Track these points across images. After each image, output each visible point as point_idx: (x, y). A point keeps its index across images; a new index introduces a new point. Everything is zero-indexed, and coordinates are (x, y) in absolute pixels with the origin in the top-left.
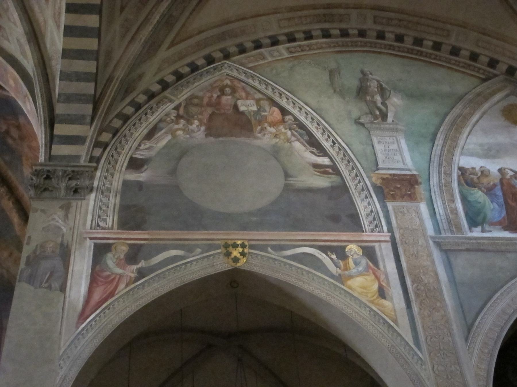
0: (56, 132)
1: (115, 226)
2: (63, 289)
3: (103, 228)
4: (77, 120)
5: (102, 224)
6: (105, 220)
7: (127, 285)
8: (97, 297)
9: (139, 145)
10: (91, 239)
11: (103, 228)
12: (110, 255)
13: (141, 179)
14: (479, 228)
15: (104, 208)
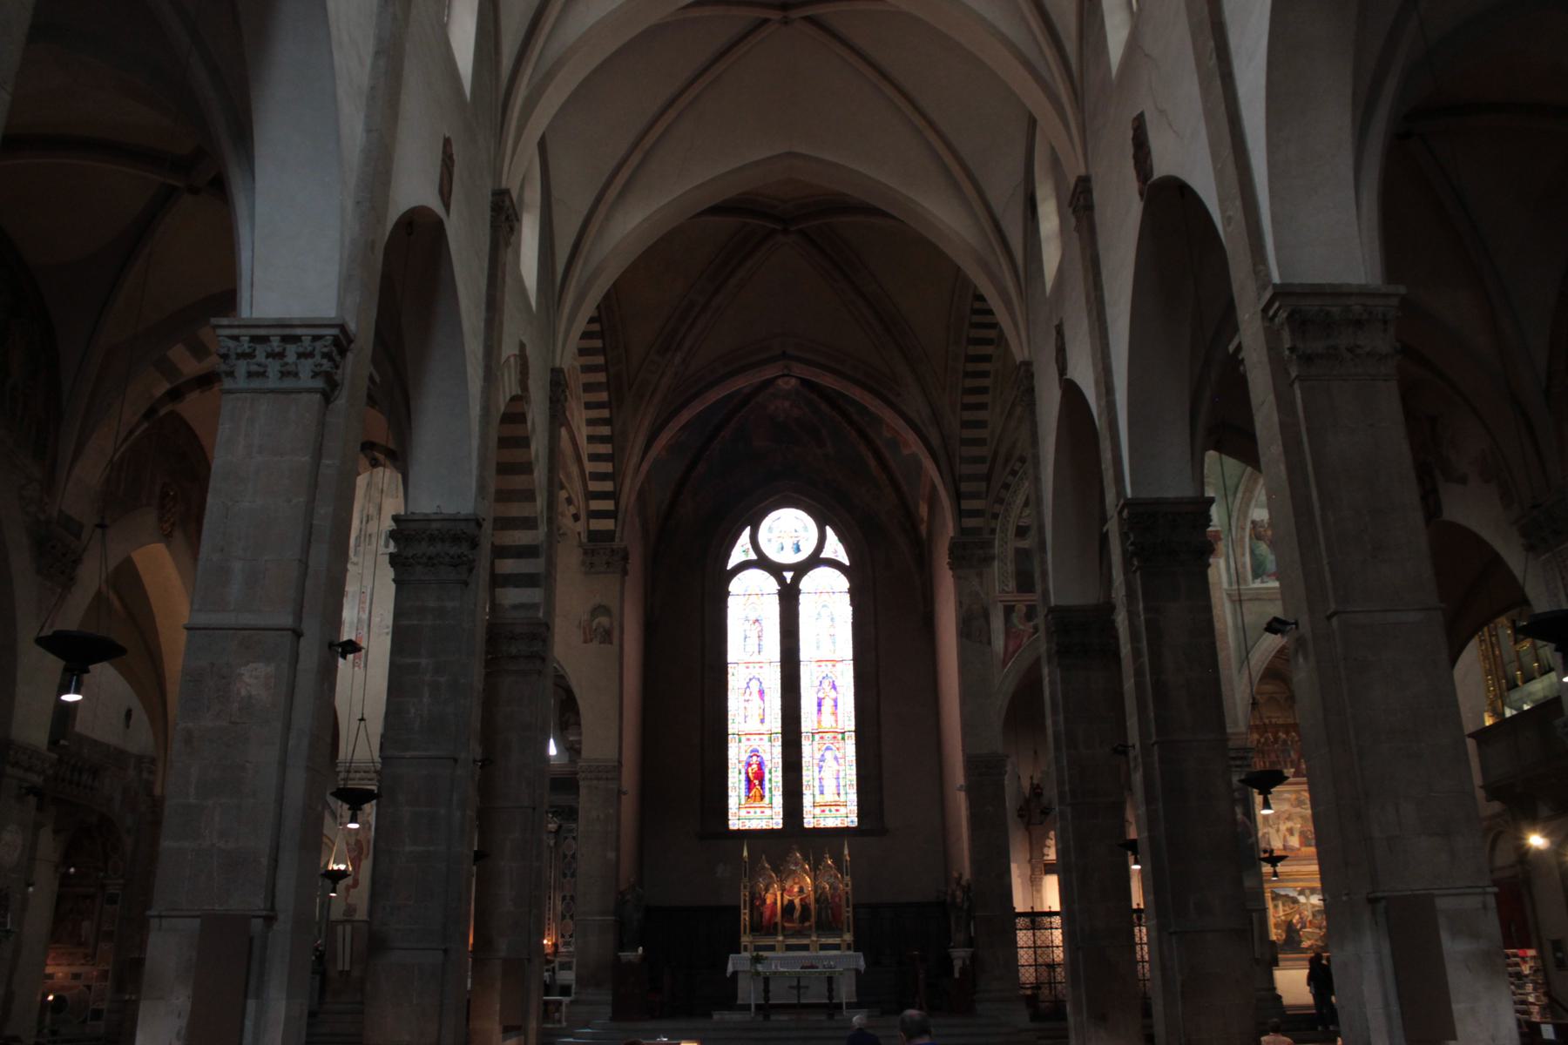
0: (963, 507)
1: (1015, 591)
2: (989, 643)
3: (1007, 592)
4: (975, 496)
5: (1006, 588)
6: (1007, 586)
7: (1029, 638)
8: (1011, 649)
9: (1021, 513)
10: (1001, 601)
11: (1007, 592)
12: (1014, 615)
13: (1026, 546)
14: (1259, 580)
15: (1005, 574)
